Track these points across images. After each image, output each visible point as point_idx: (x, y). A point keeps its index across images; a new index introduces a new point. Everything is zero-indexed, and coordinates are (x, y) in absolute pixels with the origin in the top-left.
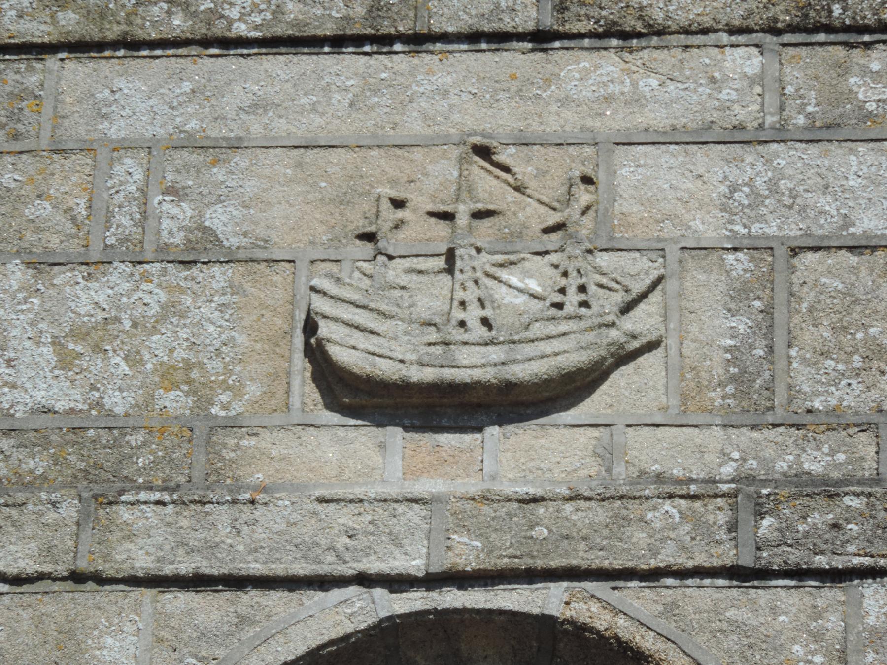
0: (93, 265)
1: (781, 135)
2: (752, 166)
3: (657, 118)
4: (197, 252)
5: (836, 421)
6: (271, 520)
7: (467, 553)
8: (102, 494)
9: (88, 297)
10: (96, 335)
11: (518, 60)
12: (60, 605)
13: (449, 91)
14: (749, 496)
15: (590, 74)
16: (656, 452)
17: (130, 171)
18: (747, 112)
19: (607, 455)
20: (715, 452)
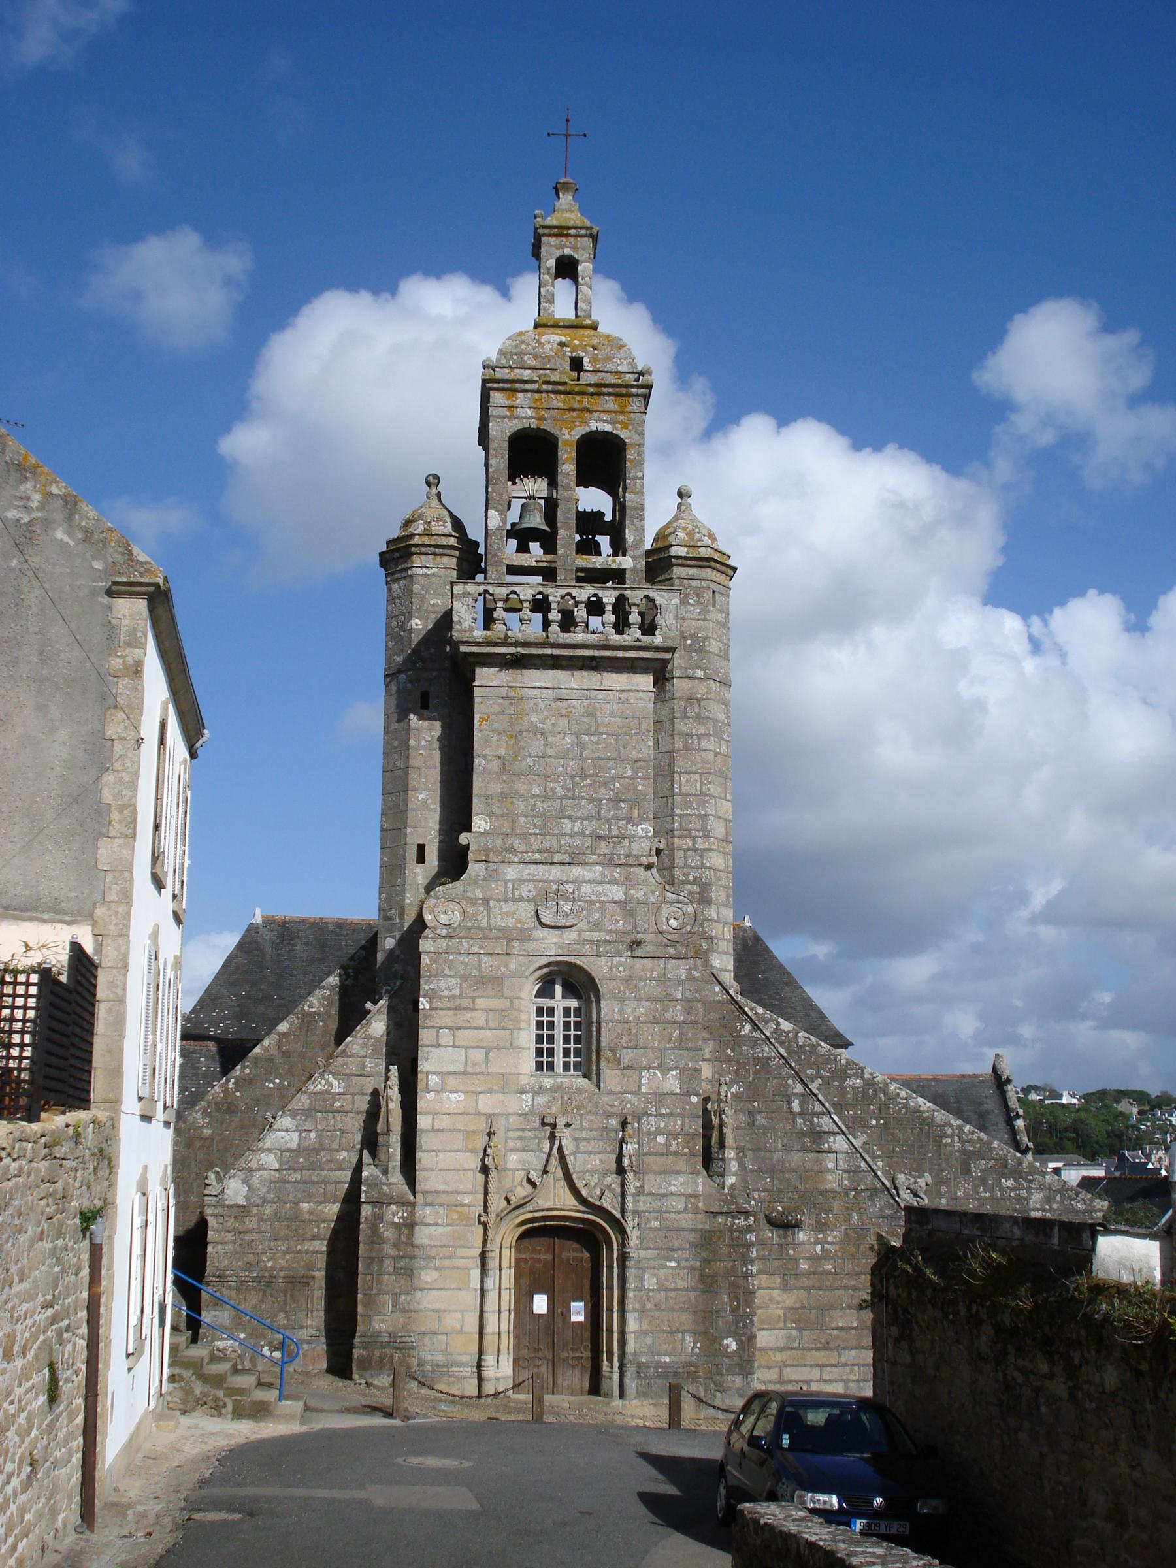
0: (506, 901)
1: (604, 882)
2: (600, 888)
3: (587, 879)
4: (521, 899)
5: (611, 931)
6: (534, 945)
7: (560, 952)
8: (510, 940)
9: (506, 907)
10: (508, 914)
11: (567, 867)
12: (504, 958)
13: (555, 872)
14: (599, 943)
15: (577, 871)
16: (587, 935)
17: (510, 885)
18: (599, 878)
19: (579, 936)
20: (597, 936)
